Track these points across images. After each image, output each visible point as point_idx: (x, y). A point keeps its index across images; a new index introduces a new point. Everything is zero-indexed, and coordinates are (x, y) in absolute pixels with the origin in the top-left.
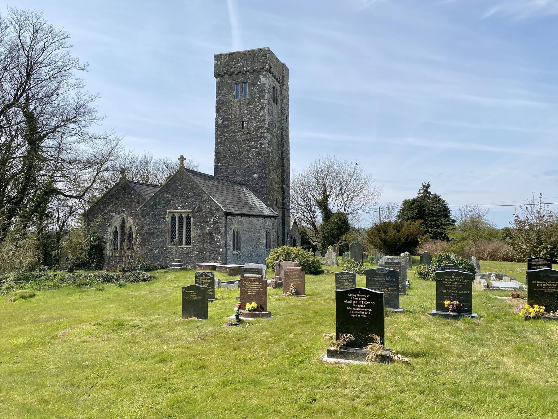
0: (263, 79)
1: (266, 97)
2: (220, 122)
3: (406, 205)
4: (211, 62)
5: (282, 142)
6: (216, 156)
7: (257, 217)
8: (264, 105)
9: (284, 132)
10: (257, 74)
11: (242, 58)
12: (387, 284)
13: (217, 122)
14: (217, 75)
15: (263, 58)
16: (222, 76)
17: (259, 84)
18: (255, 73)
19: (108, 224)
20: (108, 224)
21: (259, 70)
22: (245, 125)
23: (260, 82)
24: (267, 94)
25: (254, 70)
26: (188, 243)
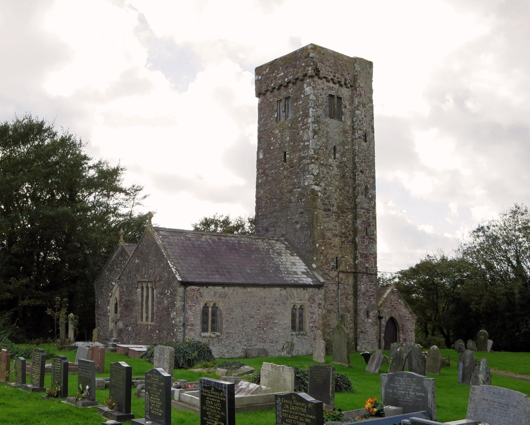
0: (308, 90)
1: (311, 113)
2: (261, 156)
3: (461, 263)
4: (251, 77)
5: (353, 173)
6: (257, 202)
7: (245, 288)
8: (308, 125)
9: (356, 157)
10: (301, 83)
11: (283, 65)
12: (308, 416)
13: (258, 156)
14: (259, 94)
15: (306, 60)
16: (264, 94)
17: (303, 96)
18: (299, 83)
19: (110, 294)
20: (110, 294)
21: (301, 77)
22: (287, 156)
23: (304, 94)
24: (311, 109)
25: (297, 79)
26: (152, 321)
